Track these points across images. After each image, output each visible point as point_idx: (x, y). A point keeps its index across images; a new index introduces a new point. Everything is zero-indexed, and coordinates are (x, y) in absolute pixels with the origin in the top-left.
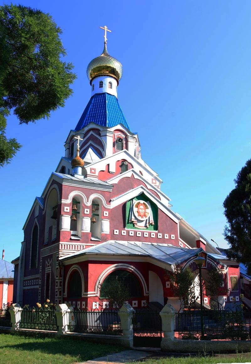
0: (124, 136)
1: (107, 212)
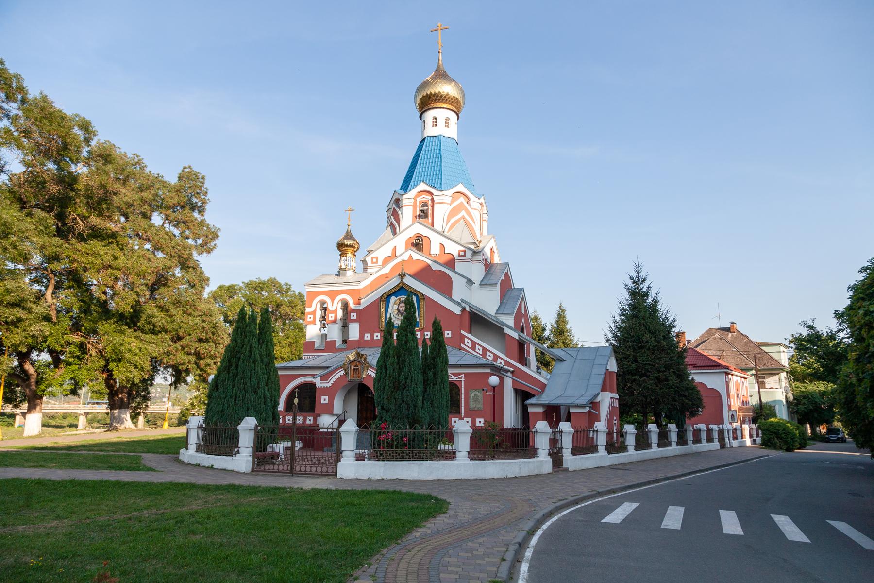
0: (430, 198)
1: (355, 314)
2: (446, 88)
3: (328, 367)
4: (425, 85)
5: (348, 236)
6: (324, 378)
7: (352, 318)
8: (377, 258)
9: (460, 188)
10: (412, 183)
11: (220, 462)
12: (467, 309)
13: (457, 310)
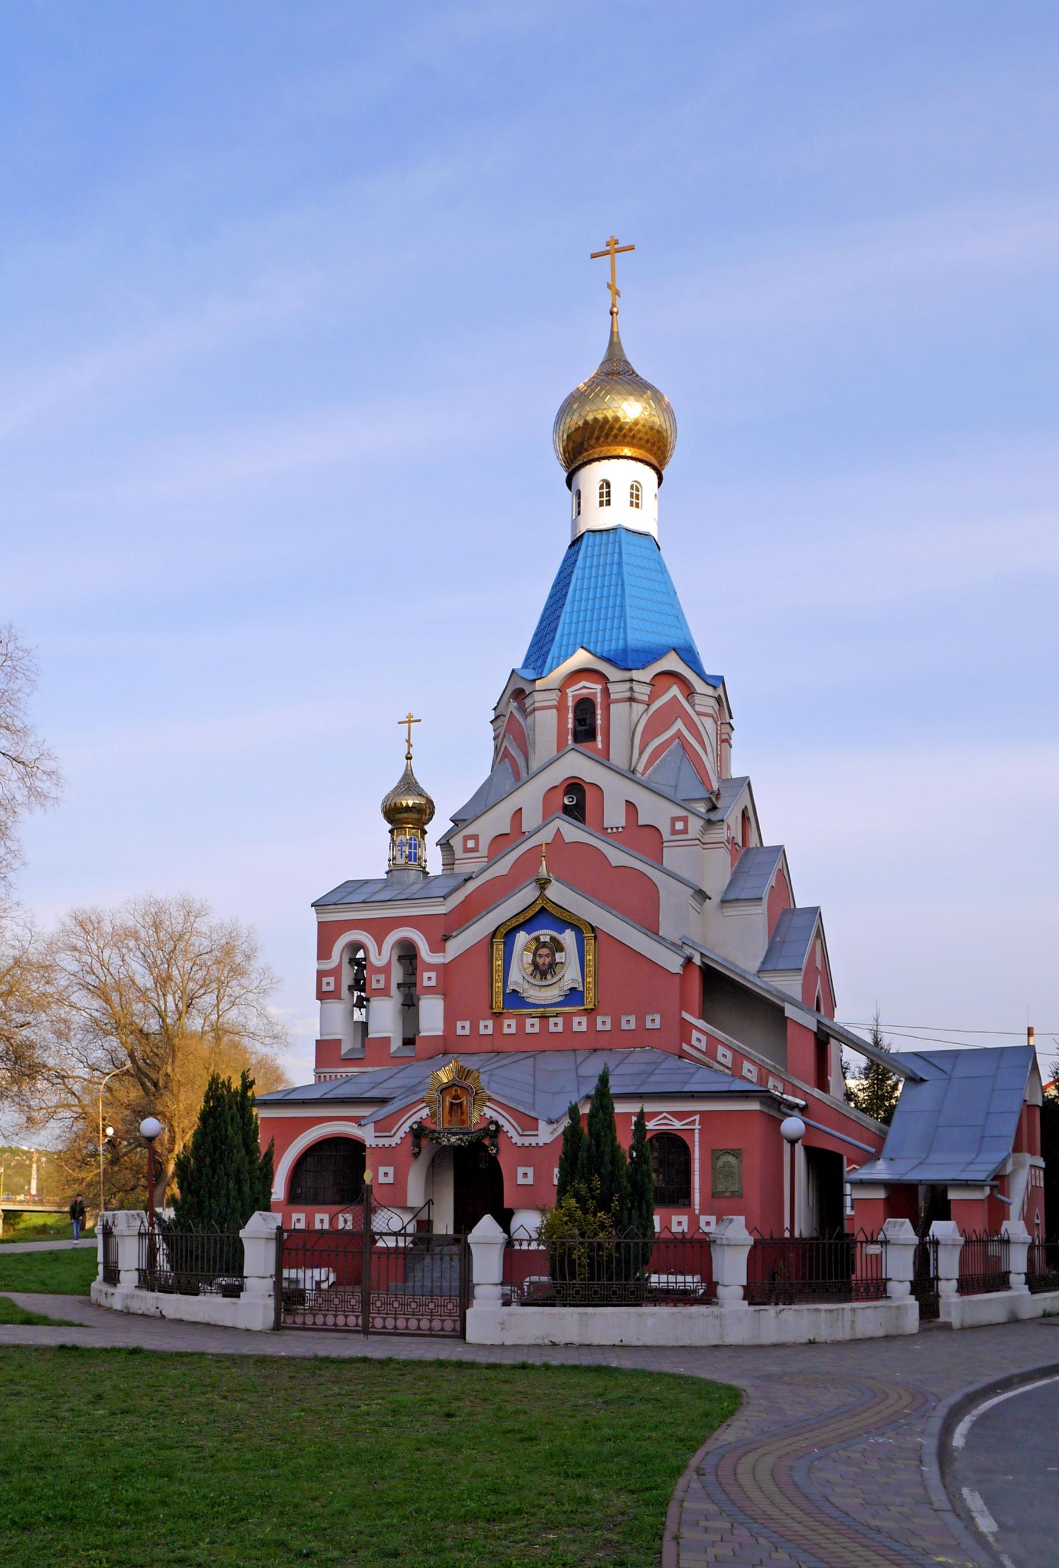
0: (598, 687)
1: (433, 975)
2: (630, 410)
3: (383, 1101)
4: (577, 399)
5: (408, 783)
6: (383, 1126)
7: (426, 983)
8: (475, 837)
9: (672, 663)
10: (554, 650)
11: (206, 1306)
12: (697, 960)
13: (673, 963)
